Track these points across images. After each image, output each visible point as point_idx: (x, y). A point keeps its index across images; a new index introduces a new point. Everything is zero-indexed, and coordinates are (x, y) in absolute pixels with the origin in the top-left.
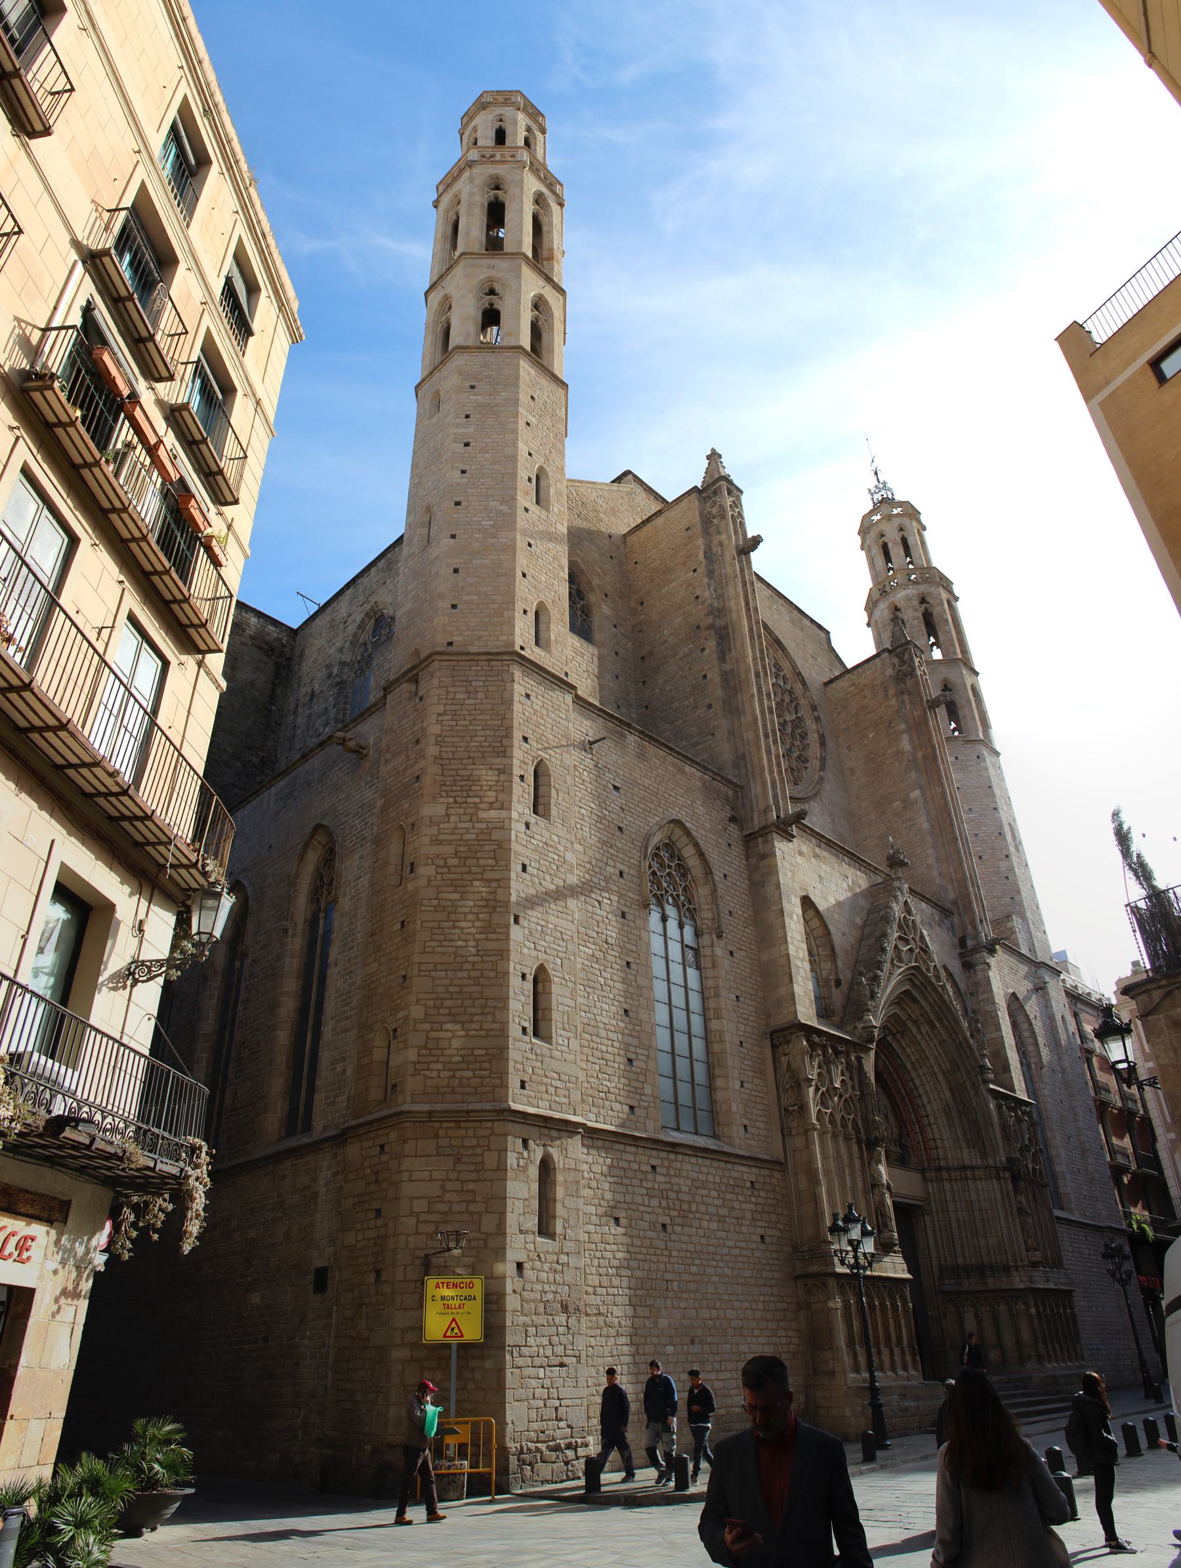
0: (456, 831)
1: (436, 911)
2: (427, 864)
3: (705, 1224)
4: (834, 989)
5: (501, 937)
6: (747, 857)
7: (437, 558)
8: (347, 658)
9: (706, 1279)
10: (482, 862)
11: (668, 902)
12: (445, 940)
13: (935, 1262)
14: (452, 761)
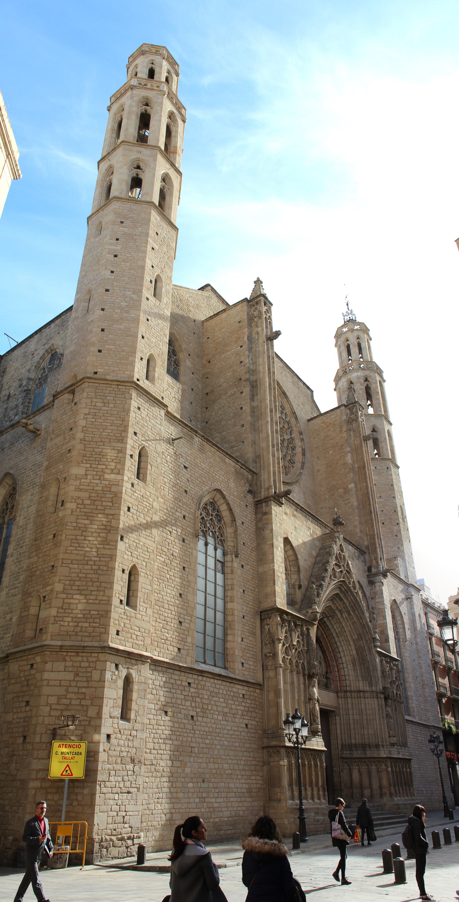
0: (90, 484)
1: (75, 529)
2: (72, 502)
3: (215, 717)
4: (297, 590)
5: (112, 547)
6: (256, 513)
8: (32, 376)
9: (213, 747)
11: (209, 535)
12: (79, 547)
13: (339, 741)
14: (91, 443)
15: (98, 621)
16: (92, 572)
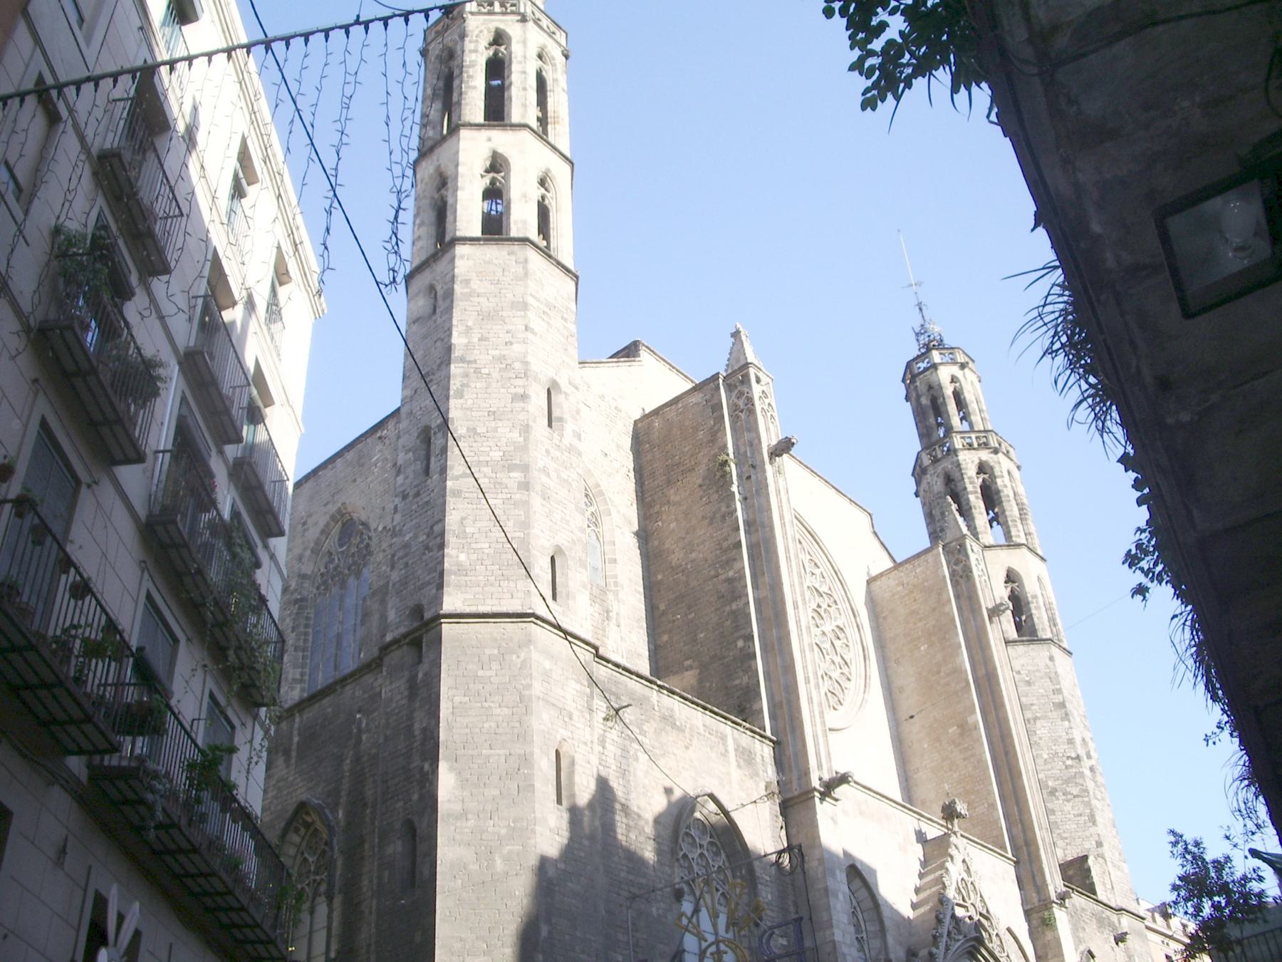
8: (308, 569)
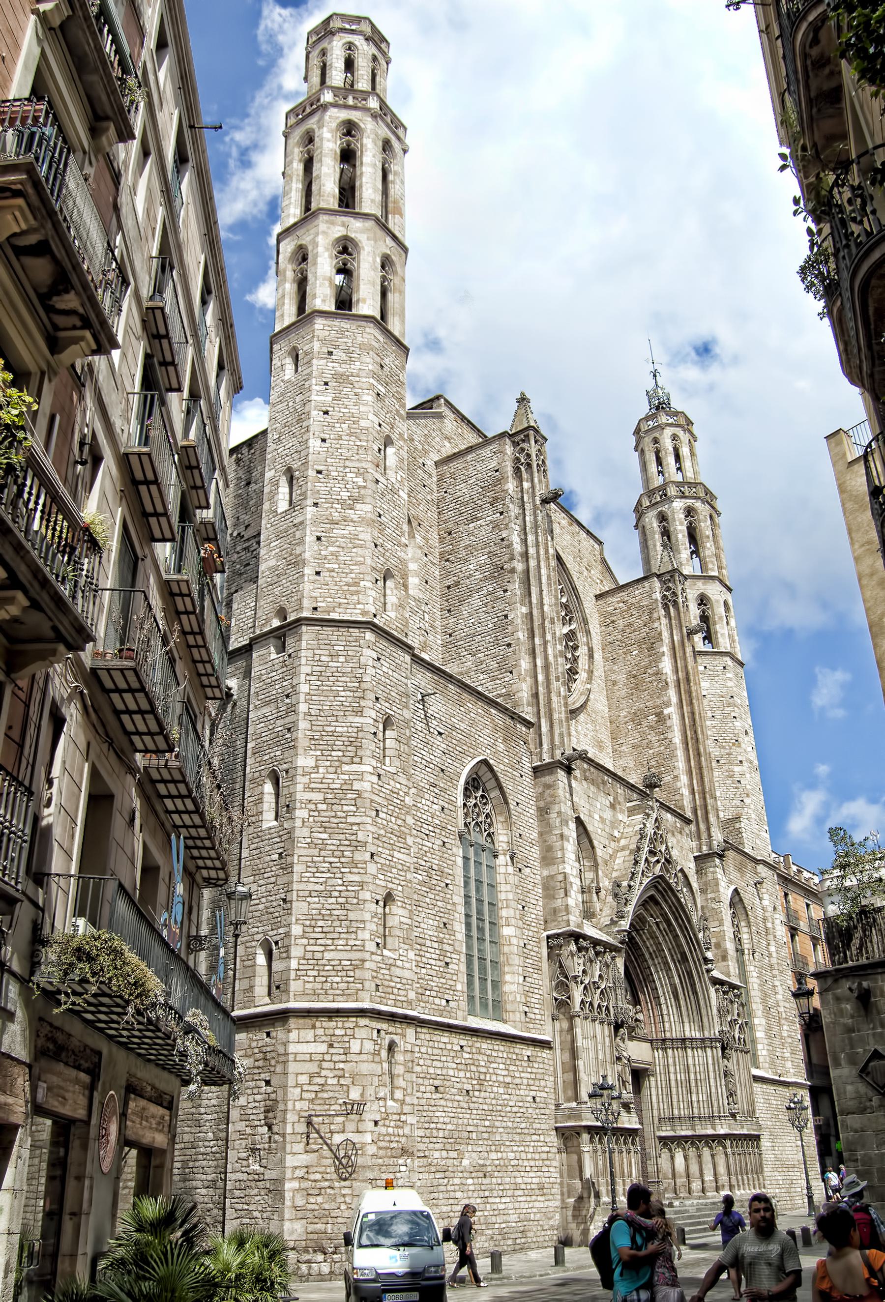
3: (495, 1089)
5: (362, 871)
7: (302, 523)
10: (345, 808)
13: (656, 1113)
15: (352, 974)
16: (338, 906)
